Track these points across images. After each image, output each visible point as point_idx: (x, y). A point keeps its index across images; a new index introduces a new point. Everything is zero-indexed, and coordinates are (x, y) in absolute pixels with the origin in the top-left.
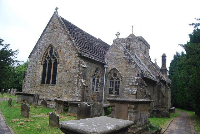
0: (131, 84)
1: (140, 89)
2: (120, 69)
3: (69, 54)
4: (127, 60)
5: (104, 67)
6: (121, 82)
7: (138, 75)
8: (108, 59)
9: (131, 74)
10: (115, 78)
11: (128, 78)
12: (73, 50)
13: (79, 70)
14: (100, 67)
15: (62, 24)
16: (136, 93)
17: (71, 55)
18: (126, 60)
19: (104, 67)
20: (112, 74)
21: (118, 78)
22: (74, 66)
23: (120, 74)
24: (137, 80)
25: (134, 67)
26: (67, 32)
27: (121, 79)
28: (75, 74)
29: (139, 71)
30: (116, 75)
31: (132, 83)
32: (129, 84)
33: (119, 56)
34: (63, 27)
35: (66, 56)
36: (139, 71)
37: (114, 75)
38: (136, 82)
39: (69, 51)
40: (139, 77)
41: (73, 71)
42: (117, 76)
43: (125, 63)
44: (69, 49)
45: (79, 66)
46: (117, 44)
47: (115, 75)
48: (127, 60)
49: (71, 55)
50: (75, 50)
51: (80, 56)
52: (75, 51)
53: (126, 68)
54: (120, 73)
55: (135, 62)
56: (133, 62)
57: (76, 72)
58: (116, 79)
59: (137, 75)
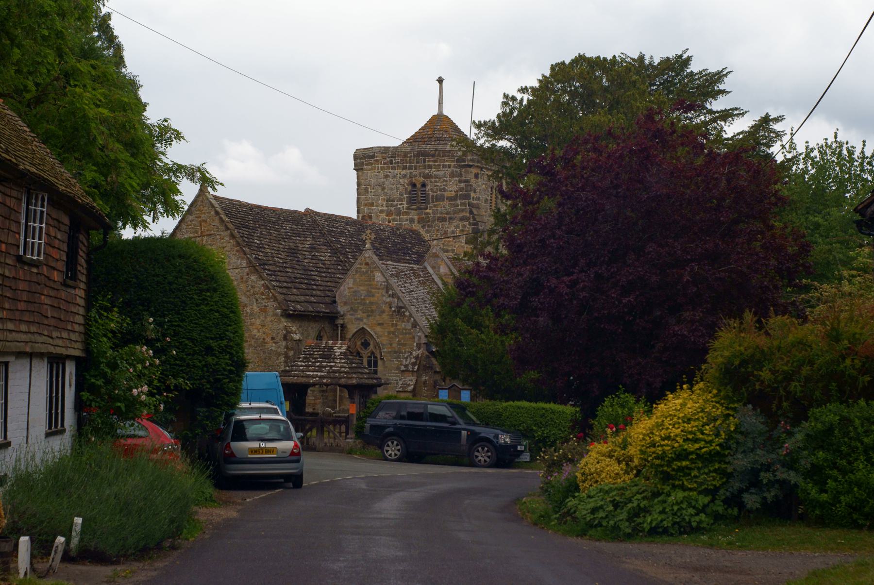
0: (403, 368)
1: (424, 378)
2: (378, 329)
3: (256, 309)
4: (393, 309)
5: (336, 323)
6: (380, 363)
7: (419, 346)
8: (345, 303)
9: (404, 345)
10: (365, 353)
11: (396, 352)
12: (267, 298)
13: (287, 347)
14: (327, 327)
15: (227, 229)
16: (414, 389)
17: (264, 310)
18: (391, 308)
19: (336, 323)
20: (359, 343)
21: (373, 353)
22: (273, 338)
23: (378, 344)
24: (417, 358)
25: (409, 326)
26: (245, 254)
27: (381, 355)
28: (279, 354)
29: (420, 337)
30: (369, 344)
31: (406, 366)
32: (398, 368)
33: (373, 296)
34: (232, 236)
35: (249, 311)
36: (420, 337)
37: (362, 344)
38: (414, 364)
39: (257, 300)
40: (420, 352)
41: (272, 346)
42: (371, 347)
43: (388, 315)
44: (257, 296)
45: (285, 338)
46: (367, 264)
47: (366, 344)
48: (393, 309)
49: (264, 310)
50: (274, 301)
51: (288, 315)
52: (271, 304)
53: (392, 329)
54: (378, 340)
55: (411, 316)
56: (407, 314)
57: (279, 350)
58: (369, 354)
59: (417, 346)
